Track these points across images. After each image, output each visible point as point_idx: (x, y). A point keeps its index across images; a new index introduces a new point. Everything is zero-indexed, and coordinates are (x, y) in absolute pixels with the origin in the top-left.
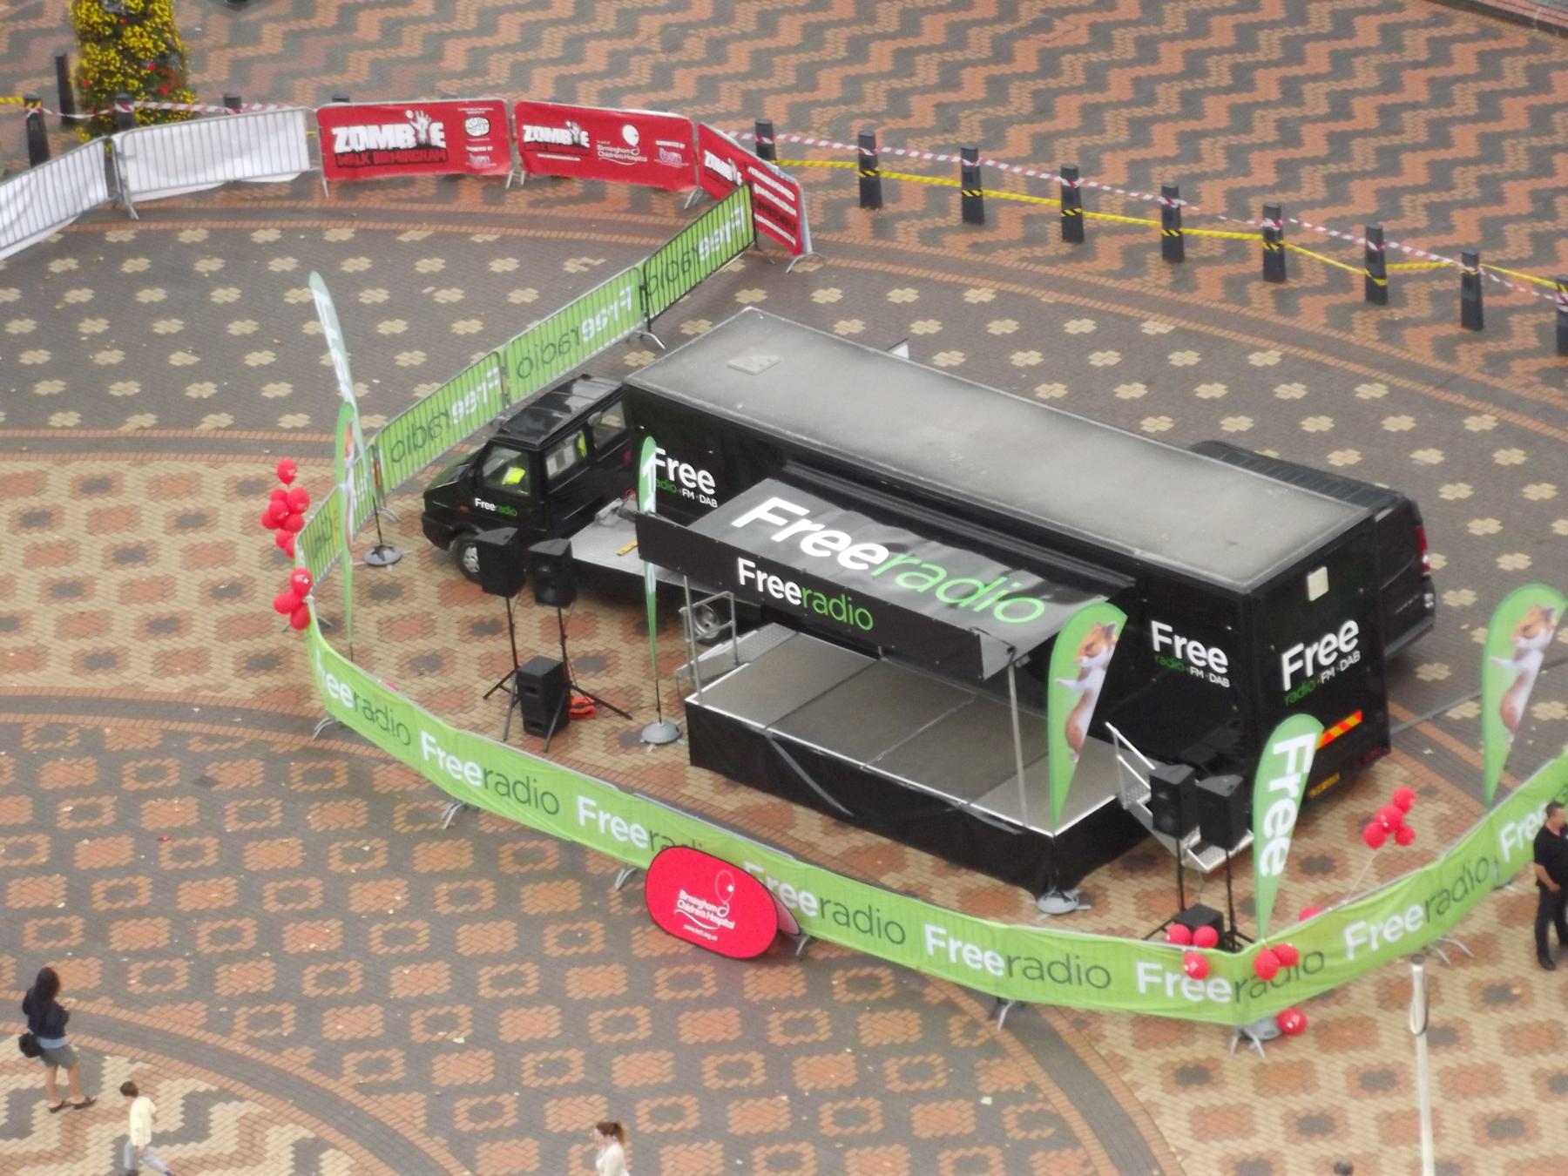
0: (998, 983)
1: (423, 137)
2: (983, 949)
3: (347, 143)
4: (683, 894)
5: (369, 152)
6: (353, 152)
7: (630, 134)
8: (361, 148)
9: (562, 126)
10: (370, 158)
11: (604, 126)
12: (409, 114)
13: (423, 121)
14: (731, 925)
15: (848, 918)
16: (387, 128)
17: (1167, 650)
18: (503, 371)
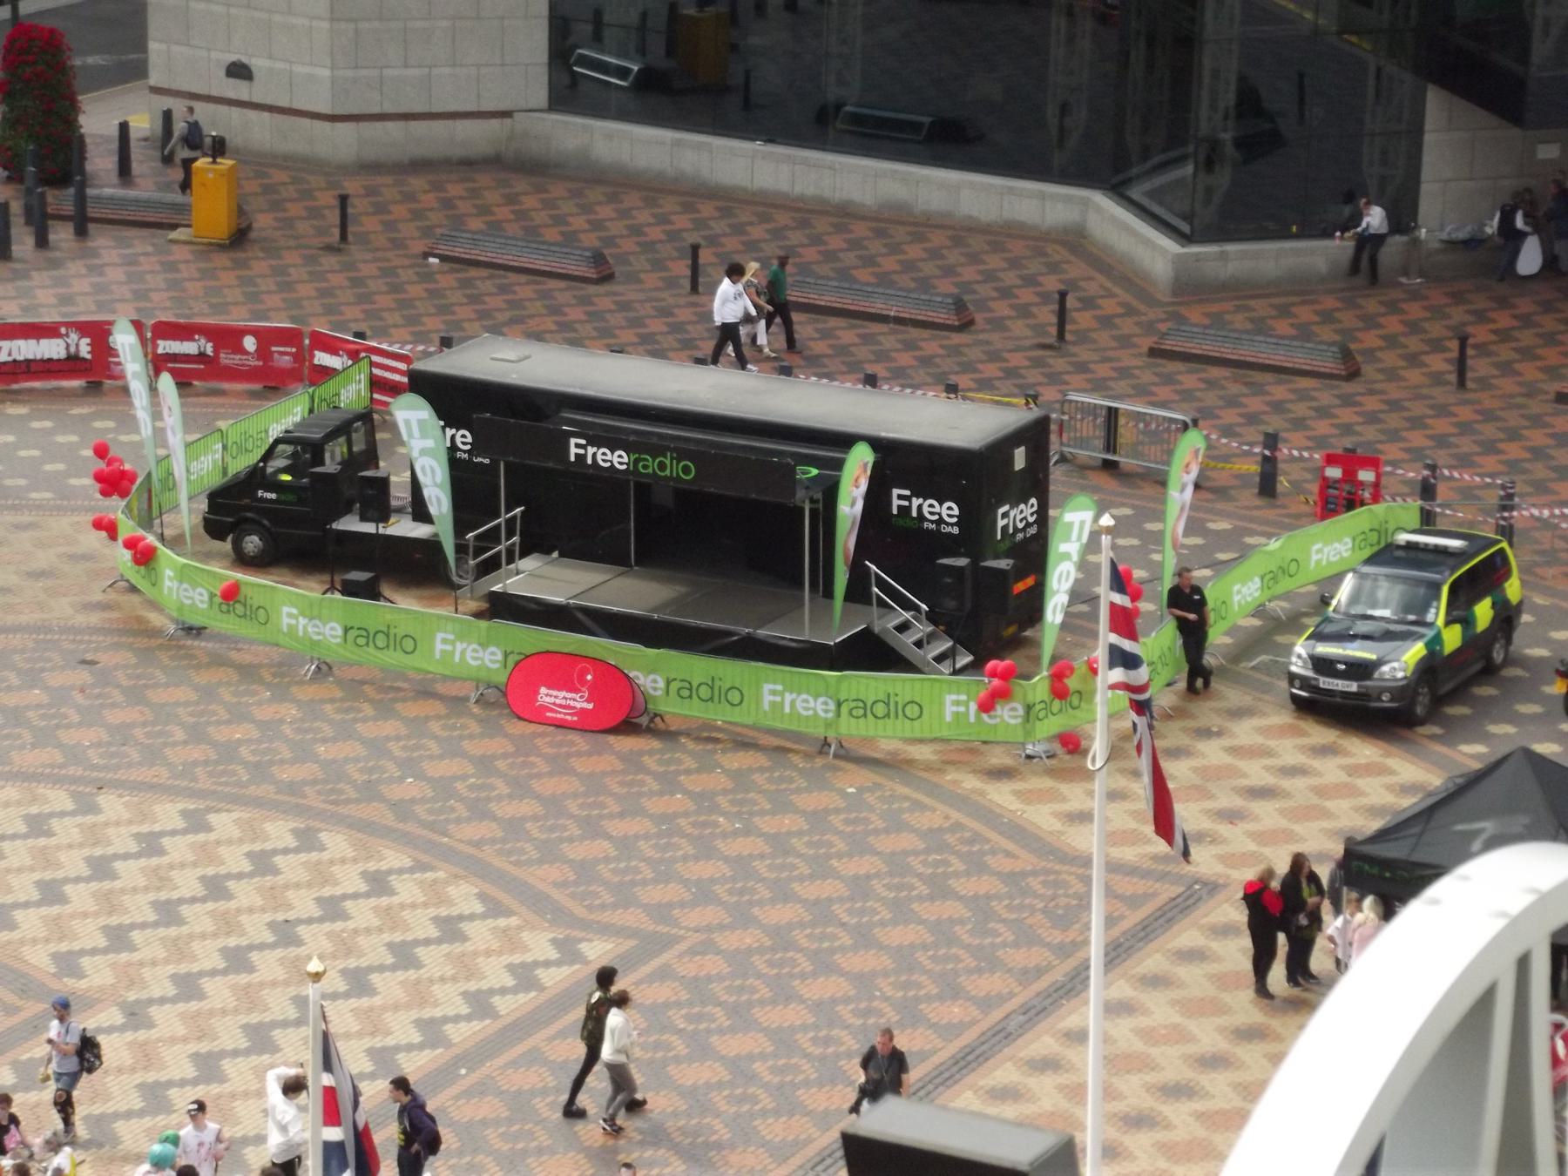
0: (828, 725)
1: (73, 350)
2: (816, 697)
3: (10, 355)
4: (543, 690)
5: (28, 361)
6: (15, 361)
7: (250, 343)
8: (21, 358)
9: (191, 339)
10: (28, 367)
11: (227, 337)
12: (63, 330)
13: (74, 337)
14: (590, 706)
15: (689, 691)
16: (44, 342)
17: (904, 511)
18: (225, 448)
